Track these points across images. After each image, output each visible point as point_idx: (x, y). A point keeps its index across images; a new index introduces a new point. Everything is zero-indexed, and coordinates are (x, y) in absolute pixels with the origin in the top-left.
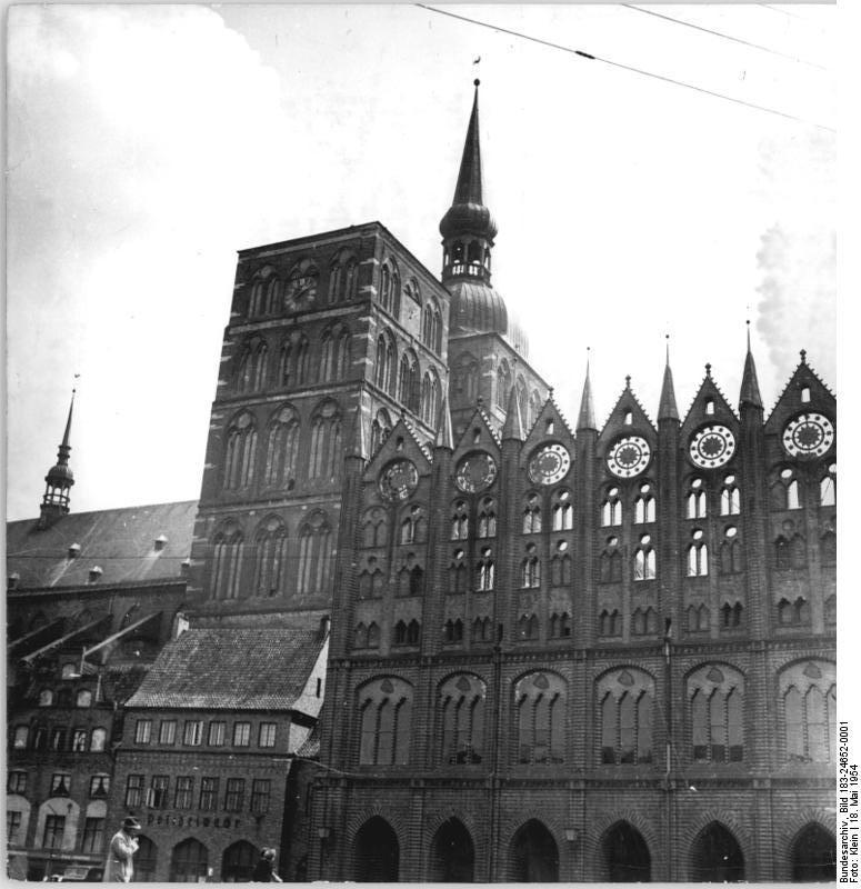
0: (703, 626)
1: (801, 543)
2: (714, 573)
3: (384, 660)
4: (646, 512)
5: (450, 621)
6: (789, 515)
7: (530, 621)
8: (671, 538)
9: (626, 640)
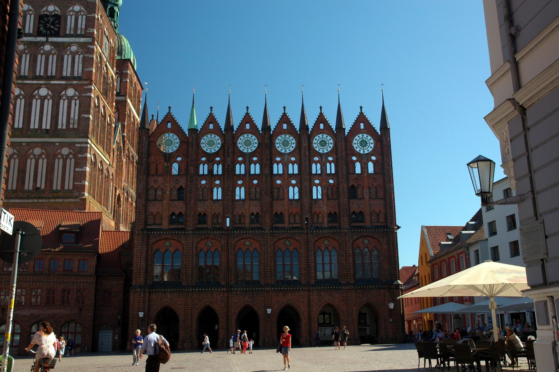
0: (320, 220)
2: (325, 198)
3: (166, 230)
4: (294, 169)
5: (200, 214)
6: (355, 176)
8: (305, 180)
9: (286, 225)
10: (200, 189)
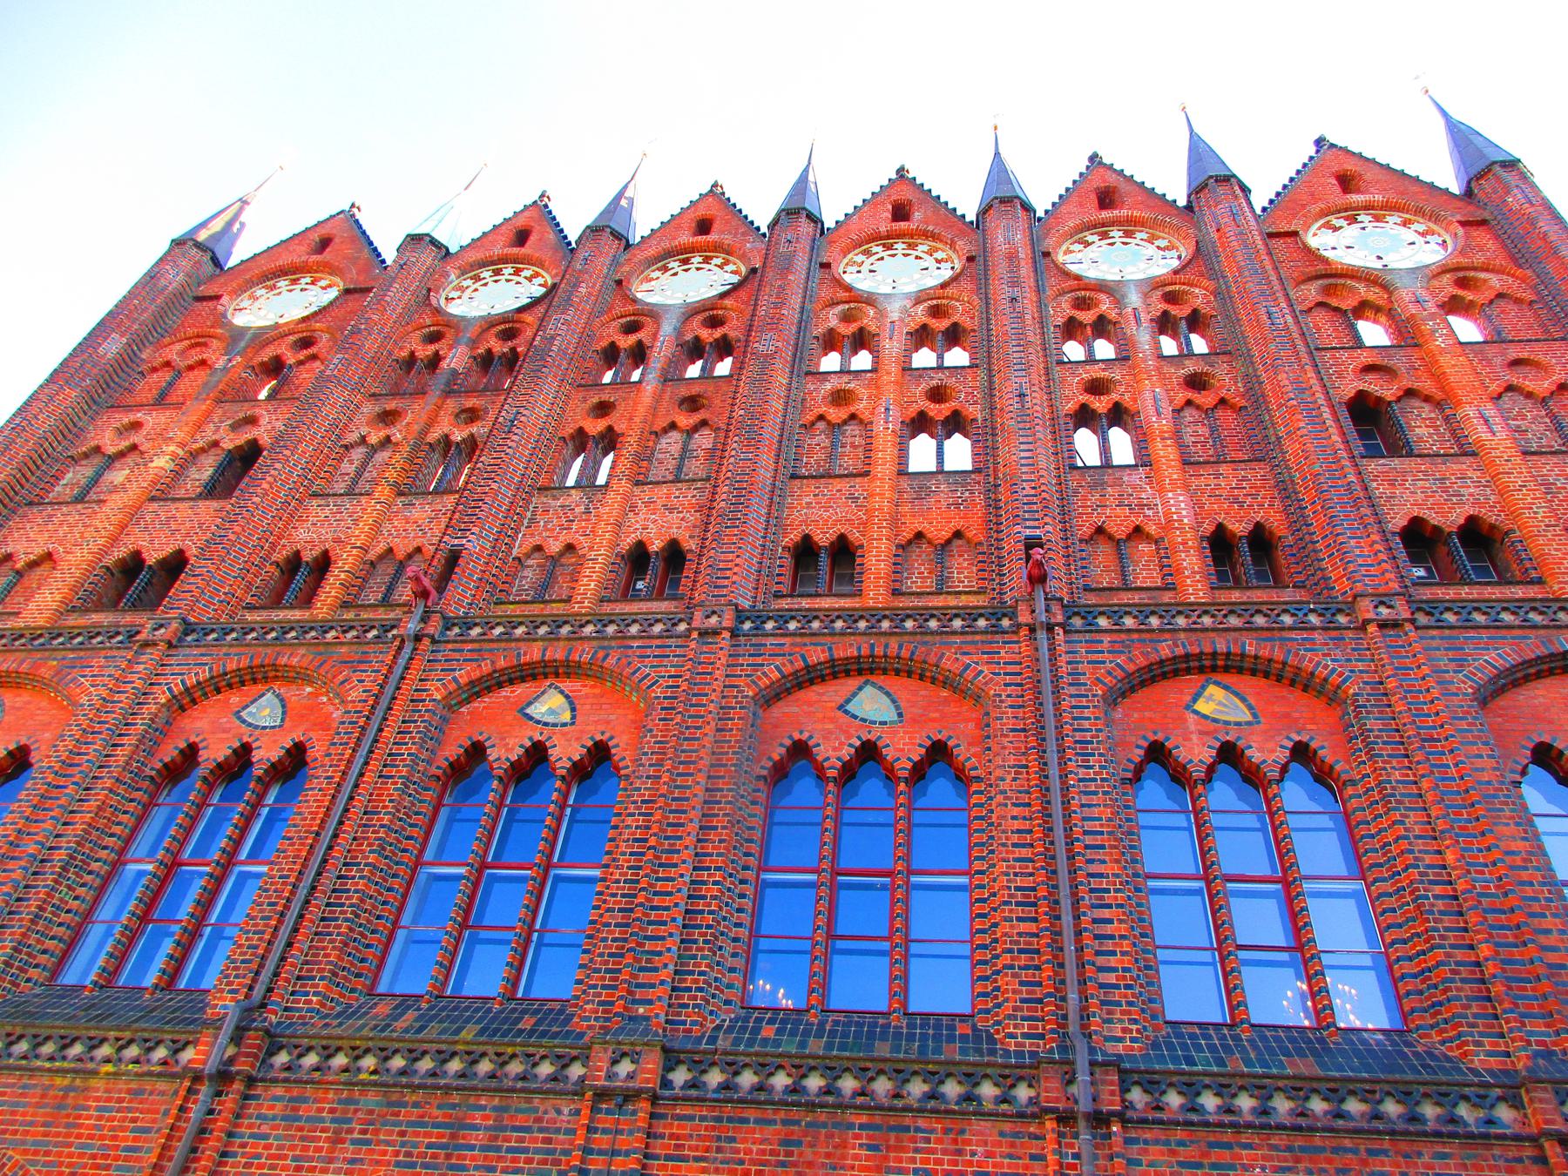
1: (1427, 410)
6: (1365, 358)
7: (554, 560)
10: (358, 454)
